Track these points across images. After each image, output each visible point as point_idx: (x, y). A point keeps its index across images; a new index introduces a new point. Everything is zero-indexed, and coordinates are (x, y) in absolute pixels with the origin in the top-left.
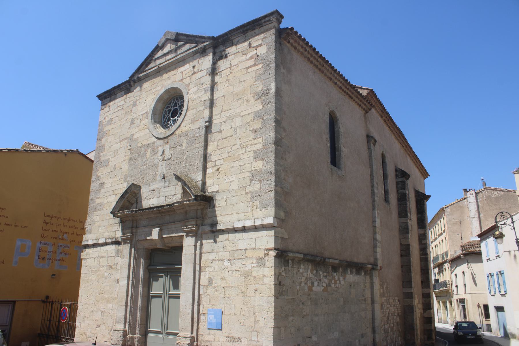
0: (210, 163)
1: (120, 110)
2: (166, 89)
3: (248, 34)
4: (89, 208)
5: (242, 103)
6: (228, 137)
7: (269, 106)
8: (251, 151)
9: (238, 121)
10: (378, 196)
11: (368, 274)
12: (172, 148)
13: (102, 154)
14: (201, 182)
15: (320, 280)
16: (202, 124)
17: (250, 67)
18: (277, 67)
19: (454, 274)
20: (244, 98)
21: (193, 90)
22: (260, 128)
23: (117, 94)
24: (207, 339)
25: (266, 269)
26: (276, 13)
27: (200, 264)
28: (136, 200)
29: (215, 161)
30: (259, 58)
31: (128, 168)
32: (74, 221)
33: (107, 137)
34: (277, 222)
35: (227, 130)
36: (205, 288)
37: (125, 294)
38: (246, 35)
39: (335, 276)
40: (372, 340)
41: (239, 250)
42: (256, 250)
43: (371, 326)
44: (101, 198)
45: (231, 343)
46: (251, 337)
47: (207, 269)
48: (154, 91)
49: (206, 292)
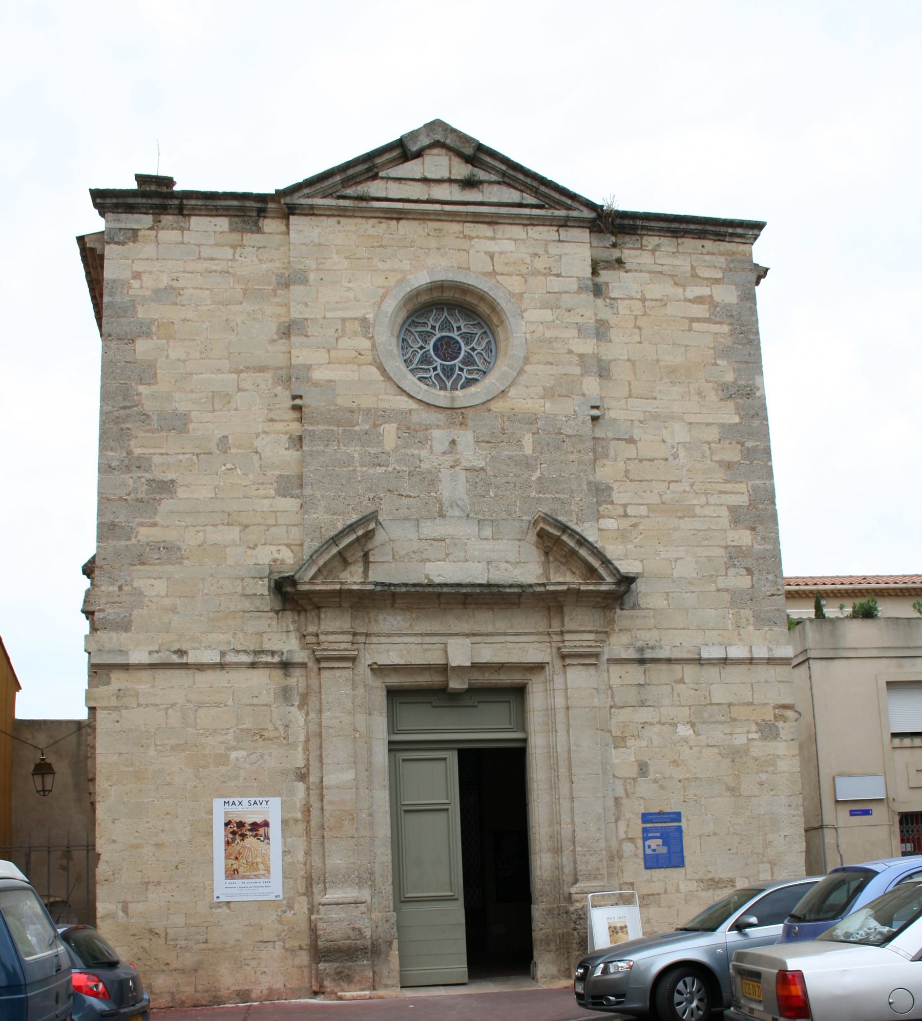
0: (609, 506)
1: (215, 271)
2: (436, 279)
6: (656, 459)
8: (721, 505)
12: (483, 441)
23: (190, 215)
25: (782, 745)
28: (362, 554)
36: (630, 783)
41: (714, 704)
42: (754, 707)
45: (711, 892)
46: (758, 875)
47: (630, 742)
49: (632, 791)
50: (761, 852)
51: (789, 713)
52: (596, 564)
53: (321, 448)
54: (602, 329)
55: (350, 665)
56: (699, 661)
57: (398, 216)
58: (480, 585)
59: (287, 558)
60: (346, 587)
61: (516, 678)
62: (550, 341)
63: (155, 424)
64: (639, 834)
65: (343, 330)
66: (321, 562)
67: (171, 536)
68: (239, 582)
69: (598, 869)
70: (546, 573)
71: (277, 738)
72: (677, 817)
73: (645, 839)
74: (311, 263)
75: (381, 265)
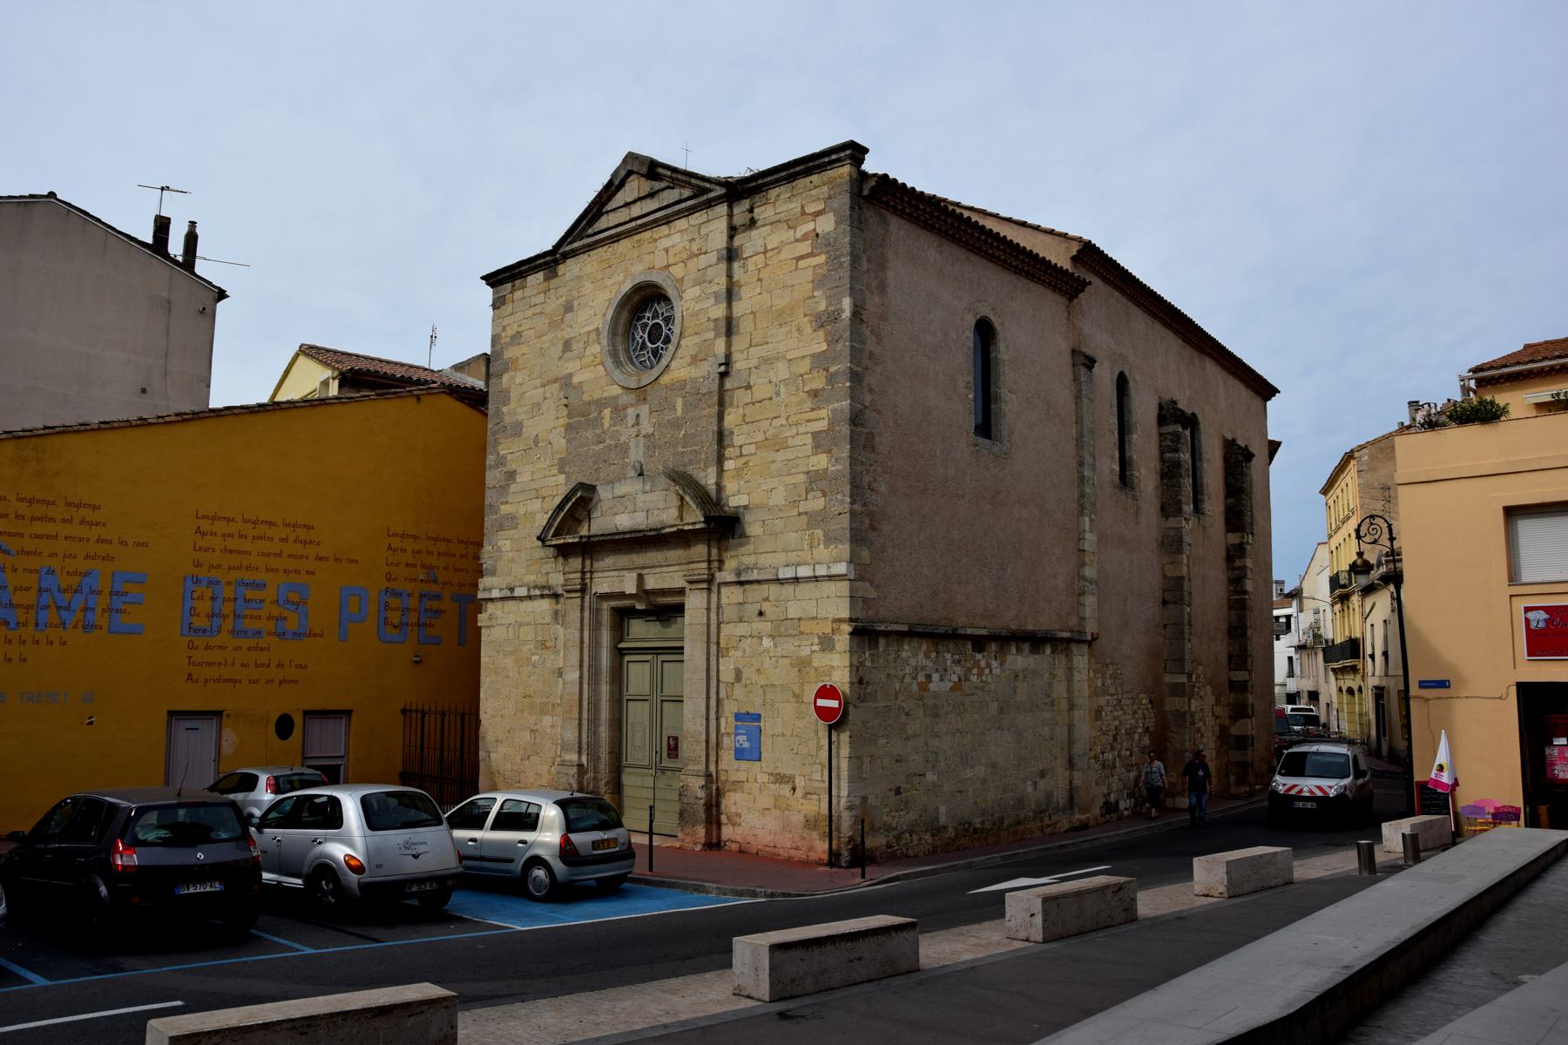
0: (731, 449)
2: (634, 284)
3: (797, 182)
4: (486, 523)
5: (788, 332)
6: (764, 400)
7: (840, 346)
9: (782, 370)
10: (1093, 484)
11: (1061, 650)
13: (504, 409)
14: (714, 487)
15: (945, 670)
16: (710, 368)
18: (855, 259)
19: (1369, 622)
20: (793, 323)
21: (691, 293)
22: (823, 390)
23: (526, 276)
24: (734, 779)
26: (852, 145)
27: (718, 644)
29: (741, 447)
30: (819, 241)
31: (564, 445)
32: (449, 541)
34: (855, 570)
37: (576, 697)
38: (794, 184)
39: (979, 660)
40: (1067, 782)
43: (1067, 756)
44: (512, 503)
45: (778, 785)
47: (732, 653)
48: (609, 282)
50: (814, 754)
55: (578, 594)
56: (778, 581)
57: (617, 238)
64: (732, 730)
71: (551, 647)
72: (758, 718)
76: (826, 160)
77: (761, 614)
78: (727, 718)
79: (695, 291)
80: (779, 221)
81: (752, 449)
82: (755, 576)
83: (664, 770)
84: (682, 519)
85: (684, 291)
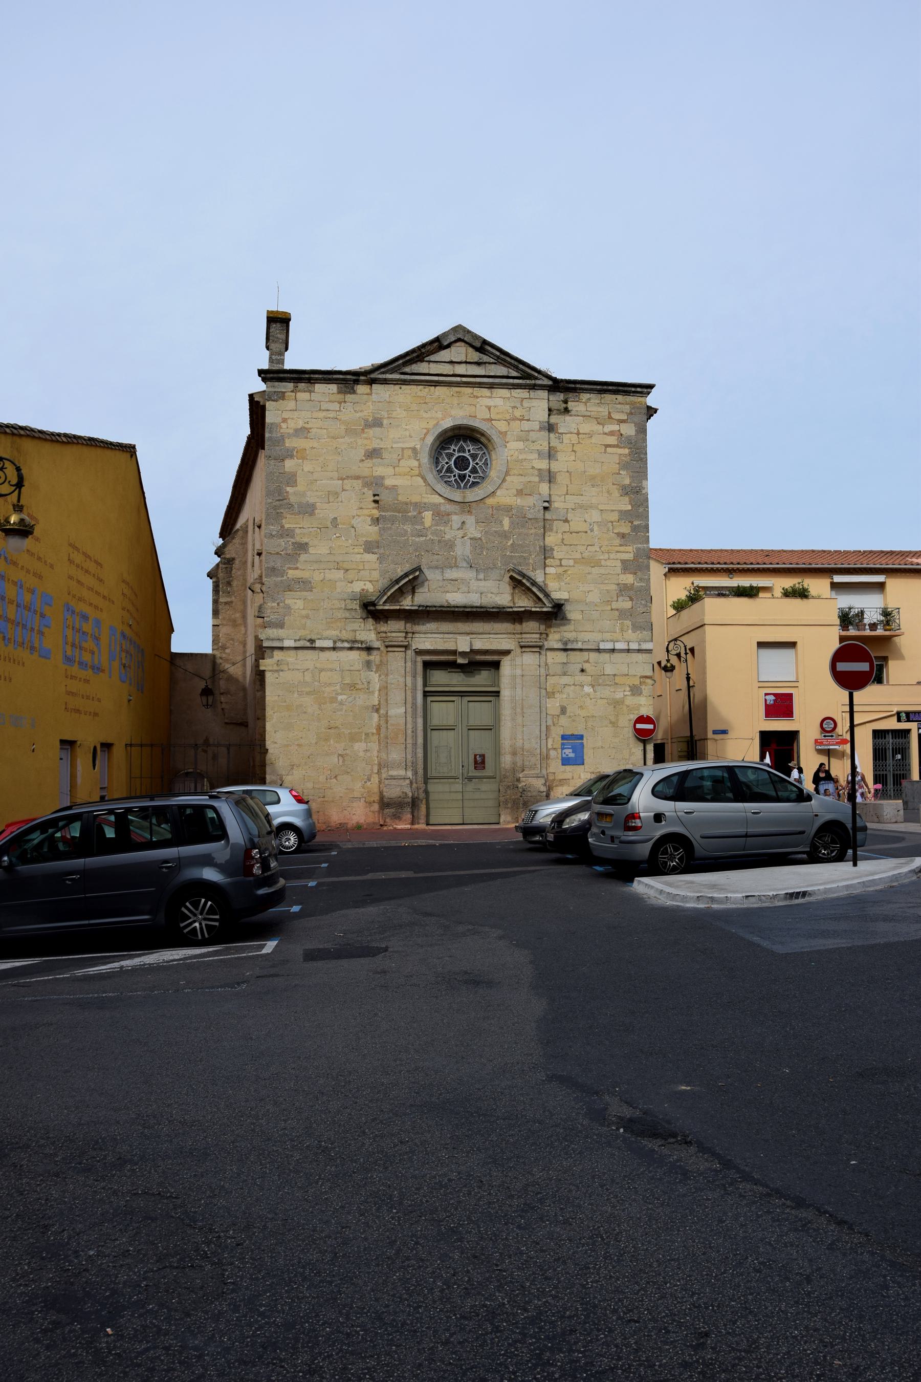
9: (595, 516)
17: (610, 446)
24: (561, 778)
33: (301, 461)
35: (577, 523)
38: (602, 396)
47: (557, 695)
51: (649, 681)
52: (541, 596)
53: (389, 526)
54: (552, 452)
55: (403, 649)
56: (598, 650)
57: (436, 384)
58: (477, 607)
59: (370, 587)
60: (402, 608)
61: (495, 658)
62: (522, 461)
63: (296, 510)
65: (403, 456)
66: (389, 594)
67: (305, 575)
68: (343, 602)
69: (535, 765)
70: (513, 600)
72: (581, 737)
73: (563, 749)
74: (385, 414)
75: (425, 415)
76: (633, 389)
77: (582, 671)
78: (554, 738)
79: (520, 445)
80: (590, 416)
81: (571, 562)
82: (579, 646)
83: (470, 779)
84: (514, 603)
85: (508, 442)
